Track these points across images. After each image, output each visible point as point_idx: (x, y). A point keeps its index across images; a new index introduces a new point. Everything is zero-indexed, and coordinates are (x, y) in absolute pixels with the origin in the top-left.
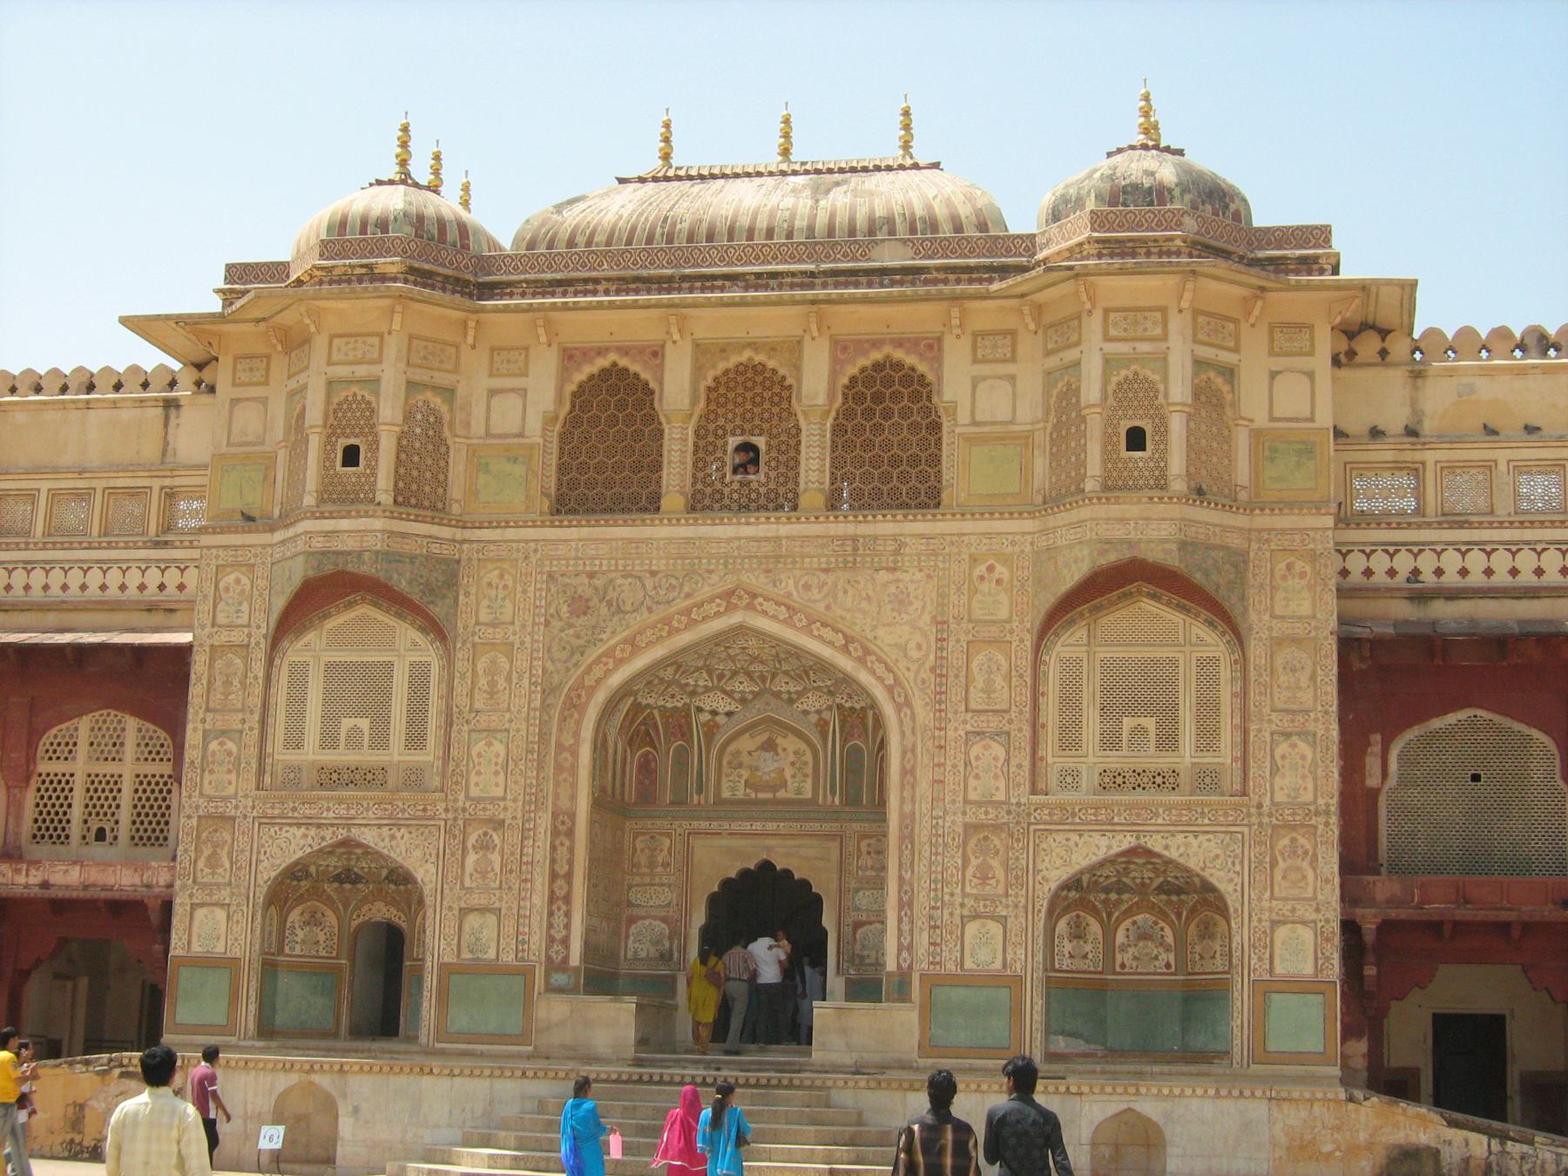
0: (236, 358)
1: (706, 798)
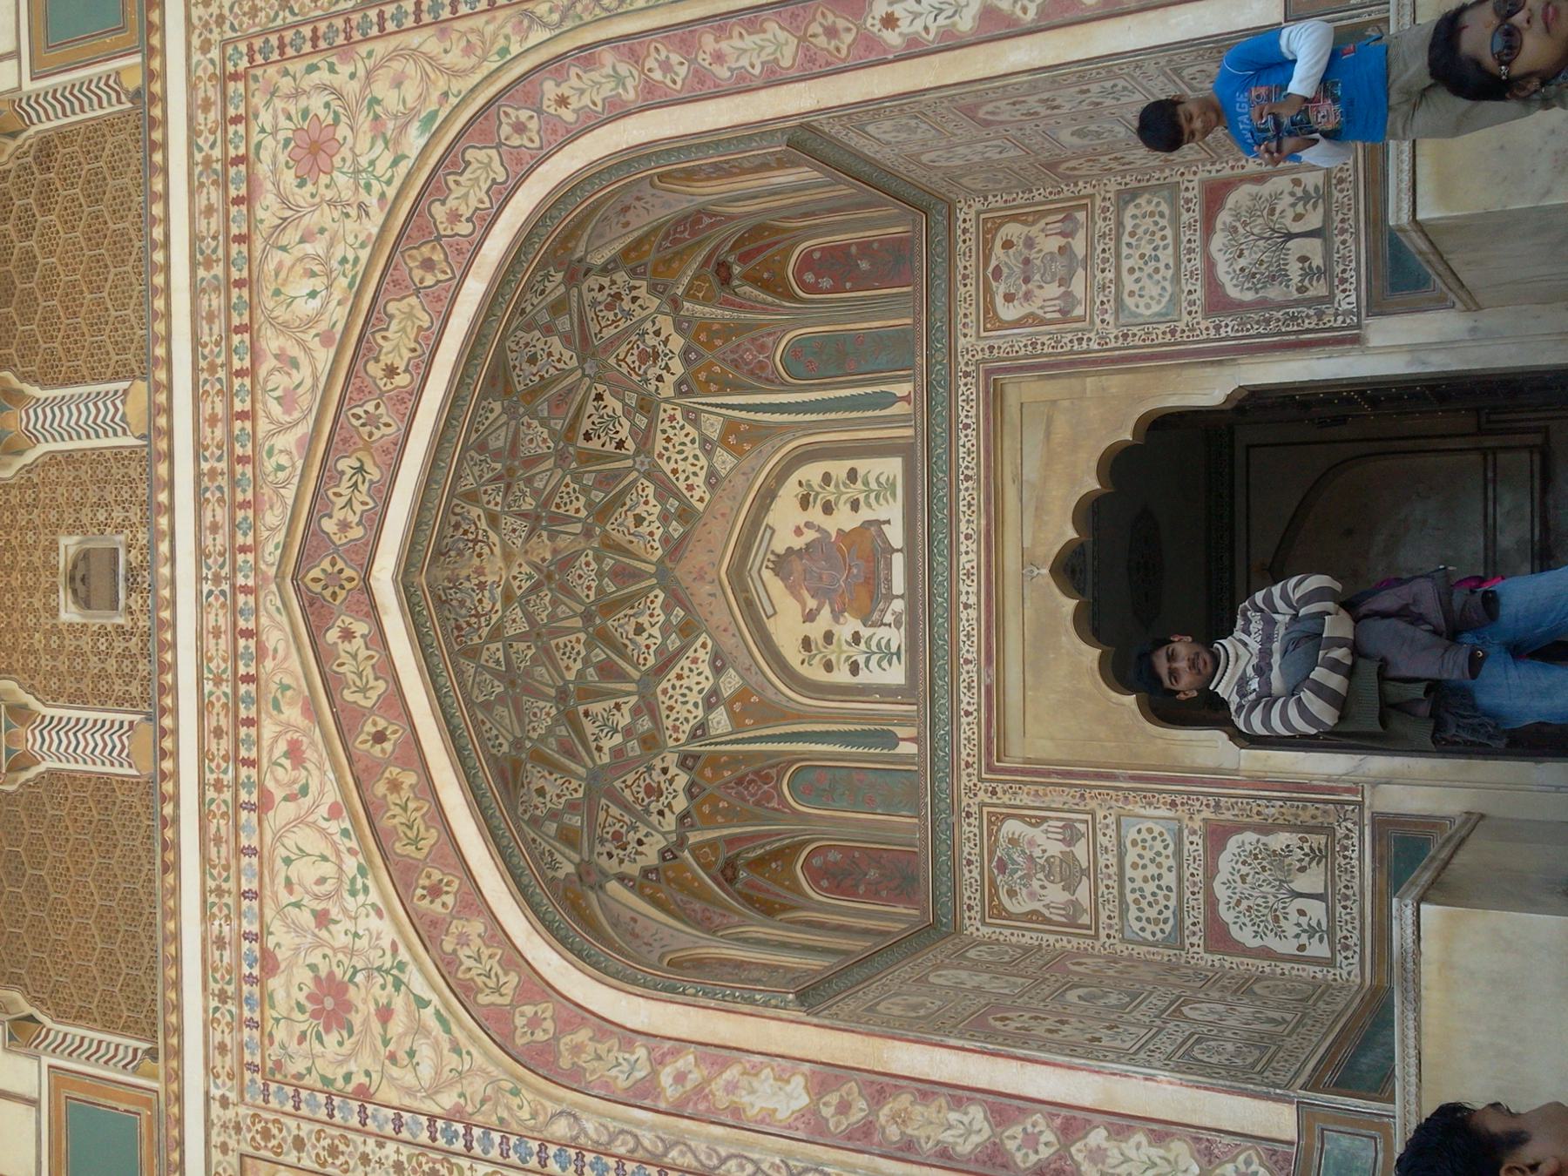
1: (904, 720)
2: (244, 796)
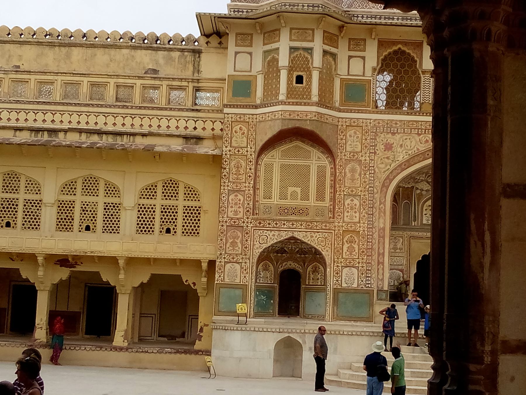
0: (237, 34)
1: (418, 223)
2: (420, 130)
